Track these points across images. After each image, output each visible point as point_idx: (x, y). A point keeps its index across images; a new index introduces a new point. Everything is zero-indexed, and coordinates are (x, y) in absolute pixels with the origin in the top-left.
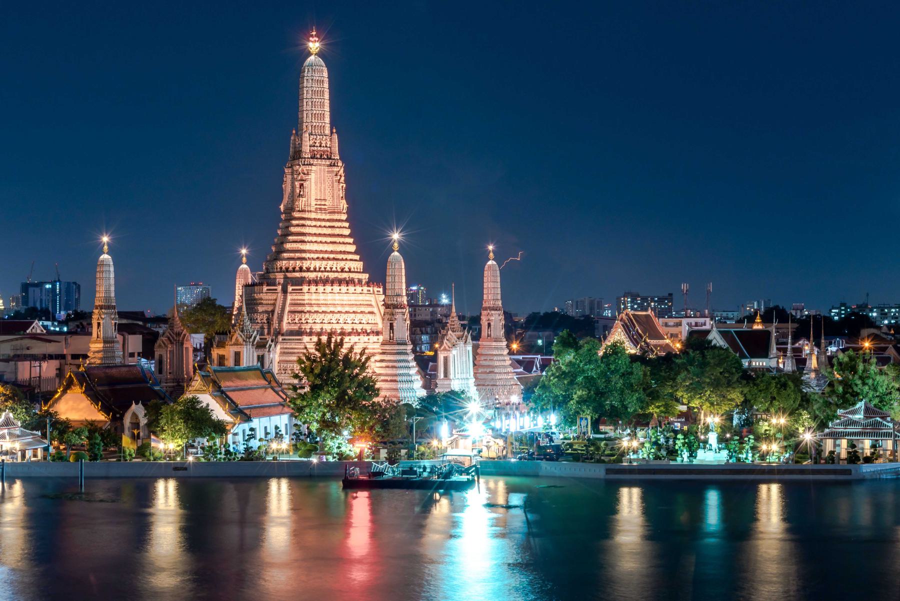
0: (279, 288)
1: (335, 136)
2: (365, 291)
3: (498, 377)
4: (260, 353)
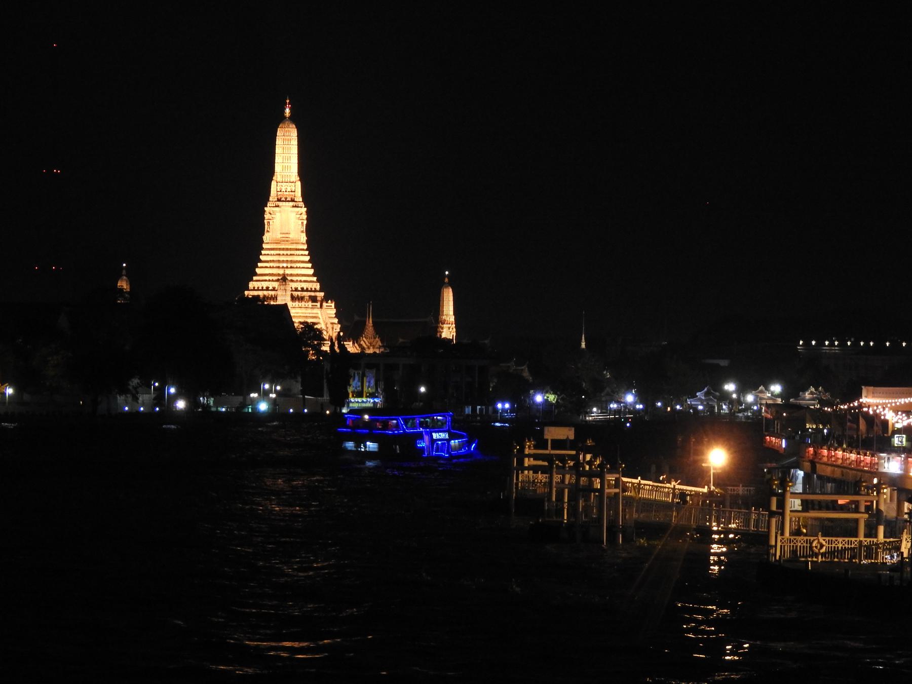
0: (318, 304)
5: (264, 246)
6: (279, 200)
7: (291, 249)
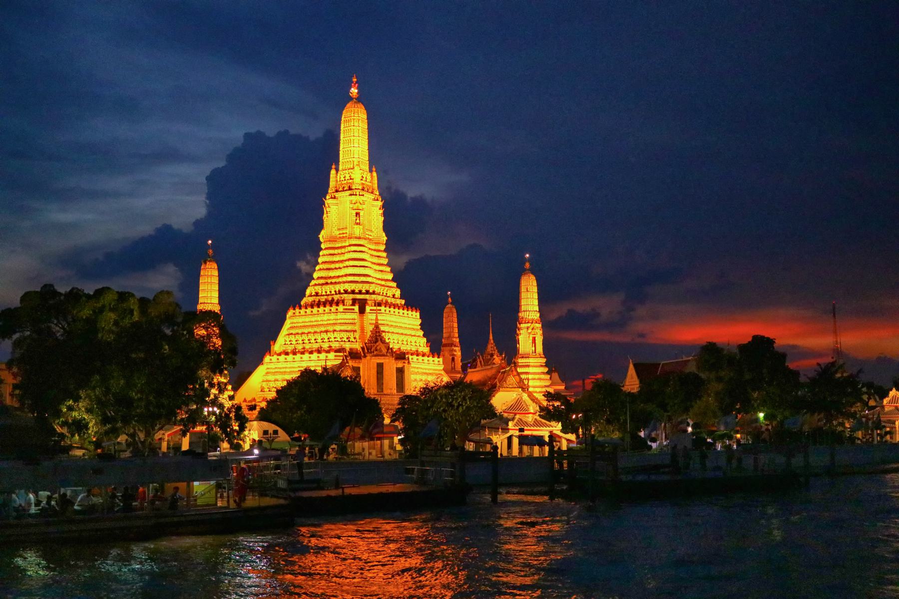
0: (356, 308)
1: (375, 174)
4: (400, 365)
5: (323, 246)
6: (337, 191)
7: (344, 247)
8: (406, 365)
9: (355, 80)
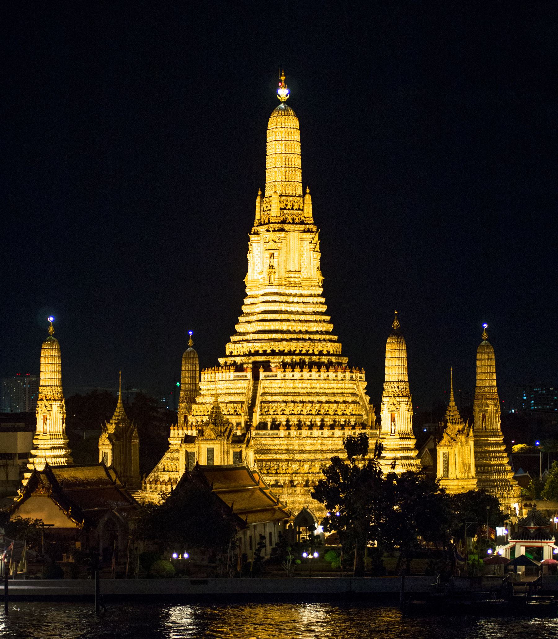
0: (249, 375)
1: (308, 197)
2: (348, 377)
3: (495, 477)
6: (261, 225)
8: (244, 449)
9: (283, 78)
